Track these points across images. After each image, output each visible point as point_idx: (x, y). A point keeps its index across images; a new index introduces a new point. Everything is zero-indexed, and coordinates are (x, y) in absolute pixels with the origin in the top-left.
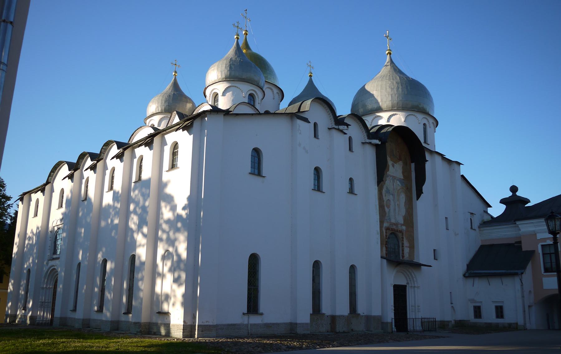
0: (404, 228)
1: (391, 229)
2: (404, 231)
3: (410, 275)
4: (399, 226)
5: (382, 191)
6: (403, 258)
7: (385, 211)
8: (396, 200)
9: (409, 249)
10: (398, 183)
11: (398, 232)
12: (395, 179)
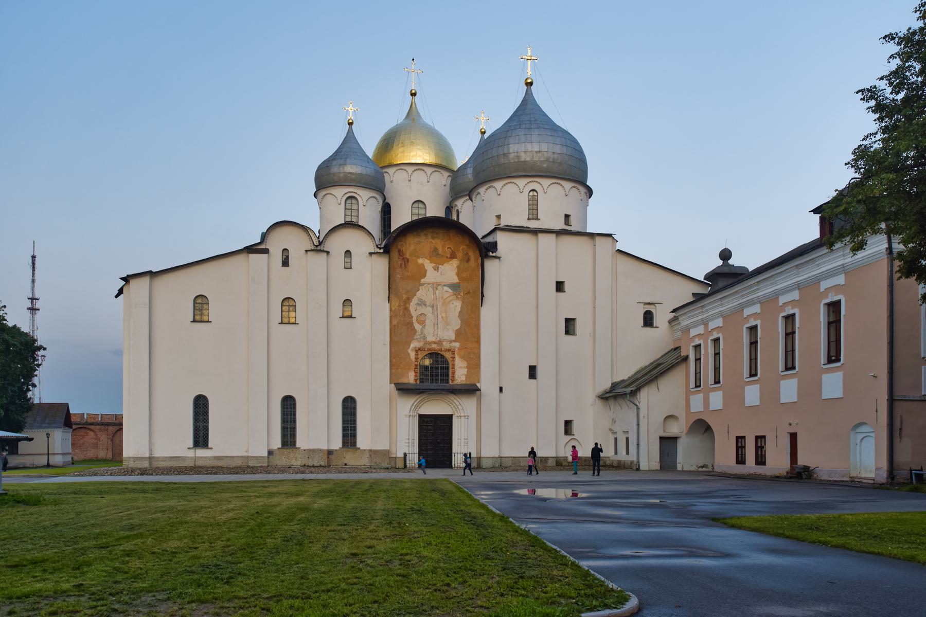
0: (457, 345)
2: (456, 349)
3: (453, 403)
4: (444, 343)
6: (452, 382)
7: (414, 329)
8: (439, 311)
9: (467, 370)
10: (446, 288)
12: (439, 285)
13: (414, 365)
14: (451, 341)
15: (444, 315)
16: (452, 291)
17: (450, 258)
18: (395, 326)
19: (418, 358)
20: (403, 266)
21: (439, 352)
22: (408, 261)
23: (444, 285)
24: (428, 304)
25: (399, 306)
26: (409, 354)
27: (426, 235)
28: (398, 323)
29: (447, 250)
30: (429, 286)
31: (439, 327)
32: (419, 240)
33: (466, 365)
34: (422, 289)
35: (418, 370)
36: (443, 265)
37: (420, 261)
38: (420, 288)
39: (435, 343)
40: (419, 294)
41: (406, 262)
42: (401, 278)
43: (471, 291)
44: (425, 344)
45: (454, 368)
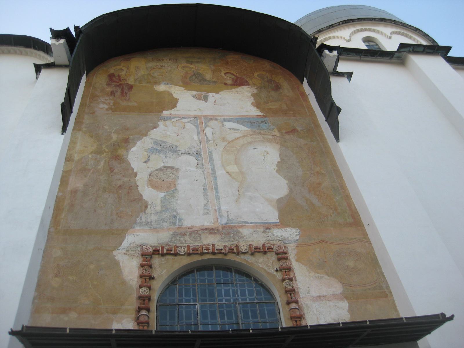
1: (182, 251)
4: (245, 232)
5: (128, 150)
7: (140, 198)
11: (238, 253)
12: (212, 119)
13: (135, 296)
14: (268, 227)
15: (233, 168)
16: (247, 129)
17: (231, 85)
18: (74, 192)
19: (152, 278)
20: (118, 93)
21: (231, 257)
22: (131, 87)
23: (225, 120)
24: (182, 149)
25: (98, 152)
26: (116, 264)
27: (176, 60)
28: (86, 185)
29: (223, 75)
30: (184, 121)
31: (221, 195)
32: (158, 64)
33: (337, 288)
34: (166, 126)
35: (153, 316)
36: (217, 92)
37: (162, 88)
38: (161, 124)
39: (212, 231)
40: (155, 134)
41: (126, 90)
42: (111, 109)
43: (299, 129)
44: (175, 235)
45: (297, 302)
